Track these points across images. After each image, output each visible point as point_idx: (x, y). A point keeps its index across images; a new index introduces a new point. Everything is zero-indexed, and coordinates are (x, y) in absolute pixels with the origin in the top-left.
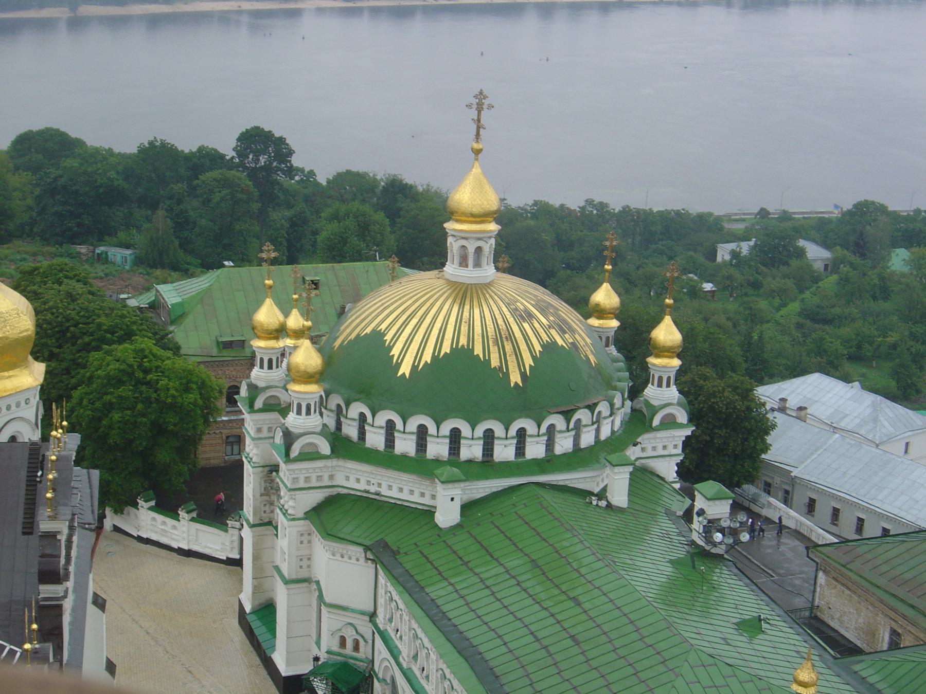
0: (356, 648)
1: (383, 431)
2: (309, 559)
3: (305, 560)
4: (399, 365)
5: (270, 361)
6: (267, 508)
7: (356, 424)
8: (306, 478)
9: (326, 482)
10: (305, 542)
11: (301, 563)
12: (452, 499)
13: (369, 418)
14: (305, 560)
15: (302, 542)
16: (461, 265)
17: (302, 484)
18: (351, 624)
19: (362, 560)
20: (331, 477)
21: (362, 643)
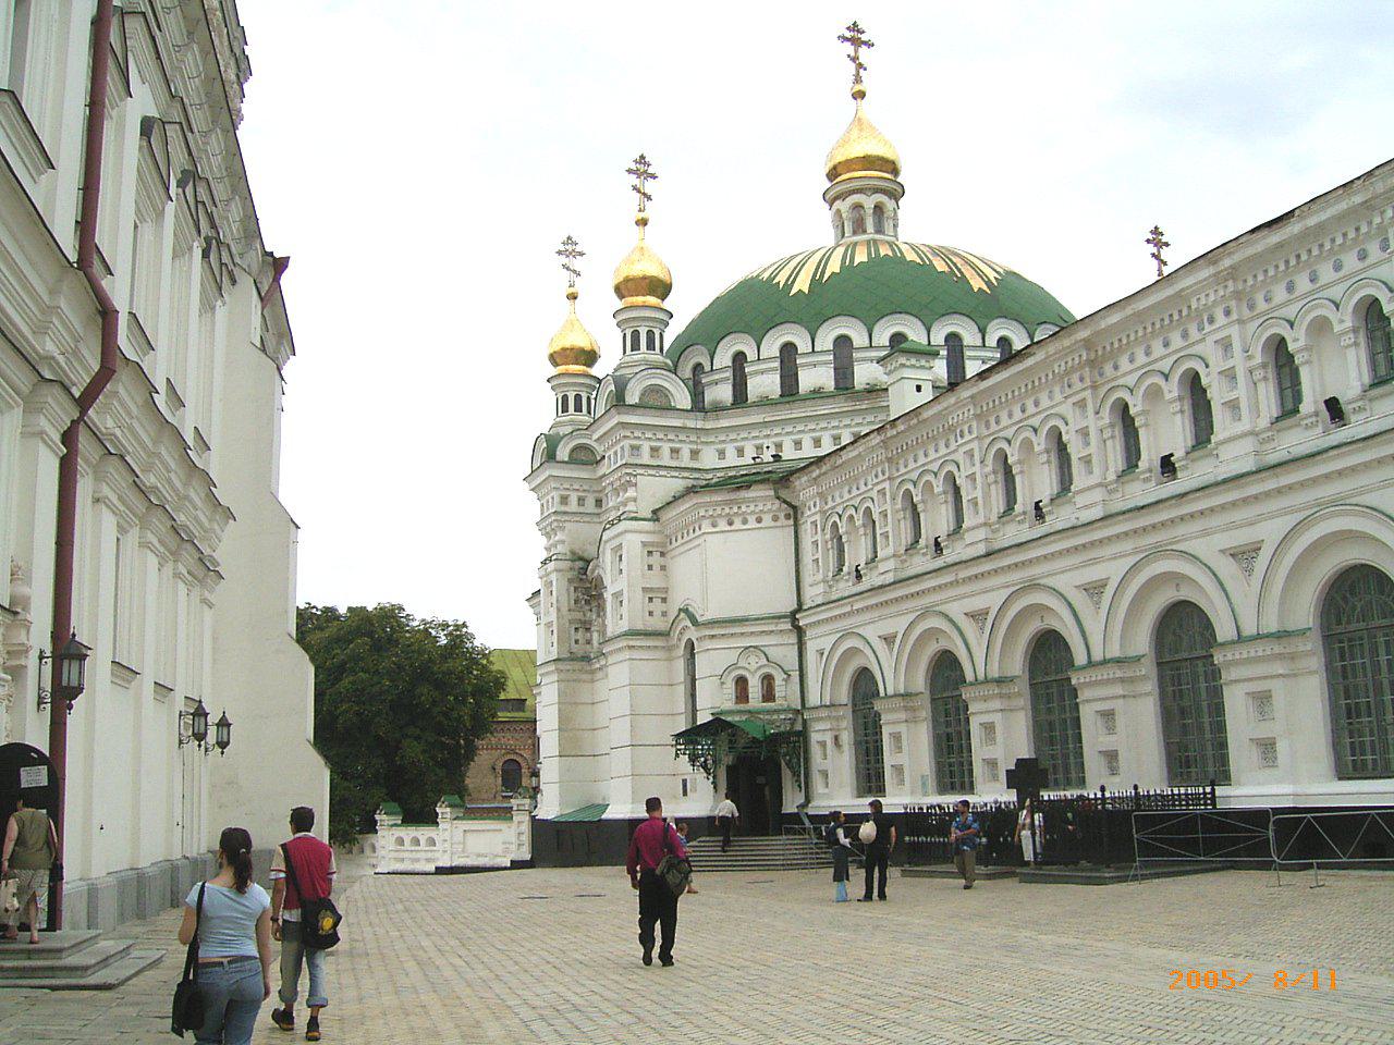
0: (769, 695)
1: (777, 364)
2: (664, 600)
3: (657, 601)
4: (788, 286)
5: (578, 398)
6: (580, 636)
7: (729, 374)
8: (652, 449)
9: (686, 461)
10: (656, 567)
11: (652, 607)
12: (919, 388)
13: (751, 355)
14: (657, 601)
15: (650, 567)
16: (855, 233)
17: (646, 459)
18: (755, 647)
19: (767, 520)
20: (695, 454)
21: (779, 678)
